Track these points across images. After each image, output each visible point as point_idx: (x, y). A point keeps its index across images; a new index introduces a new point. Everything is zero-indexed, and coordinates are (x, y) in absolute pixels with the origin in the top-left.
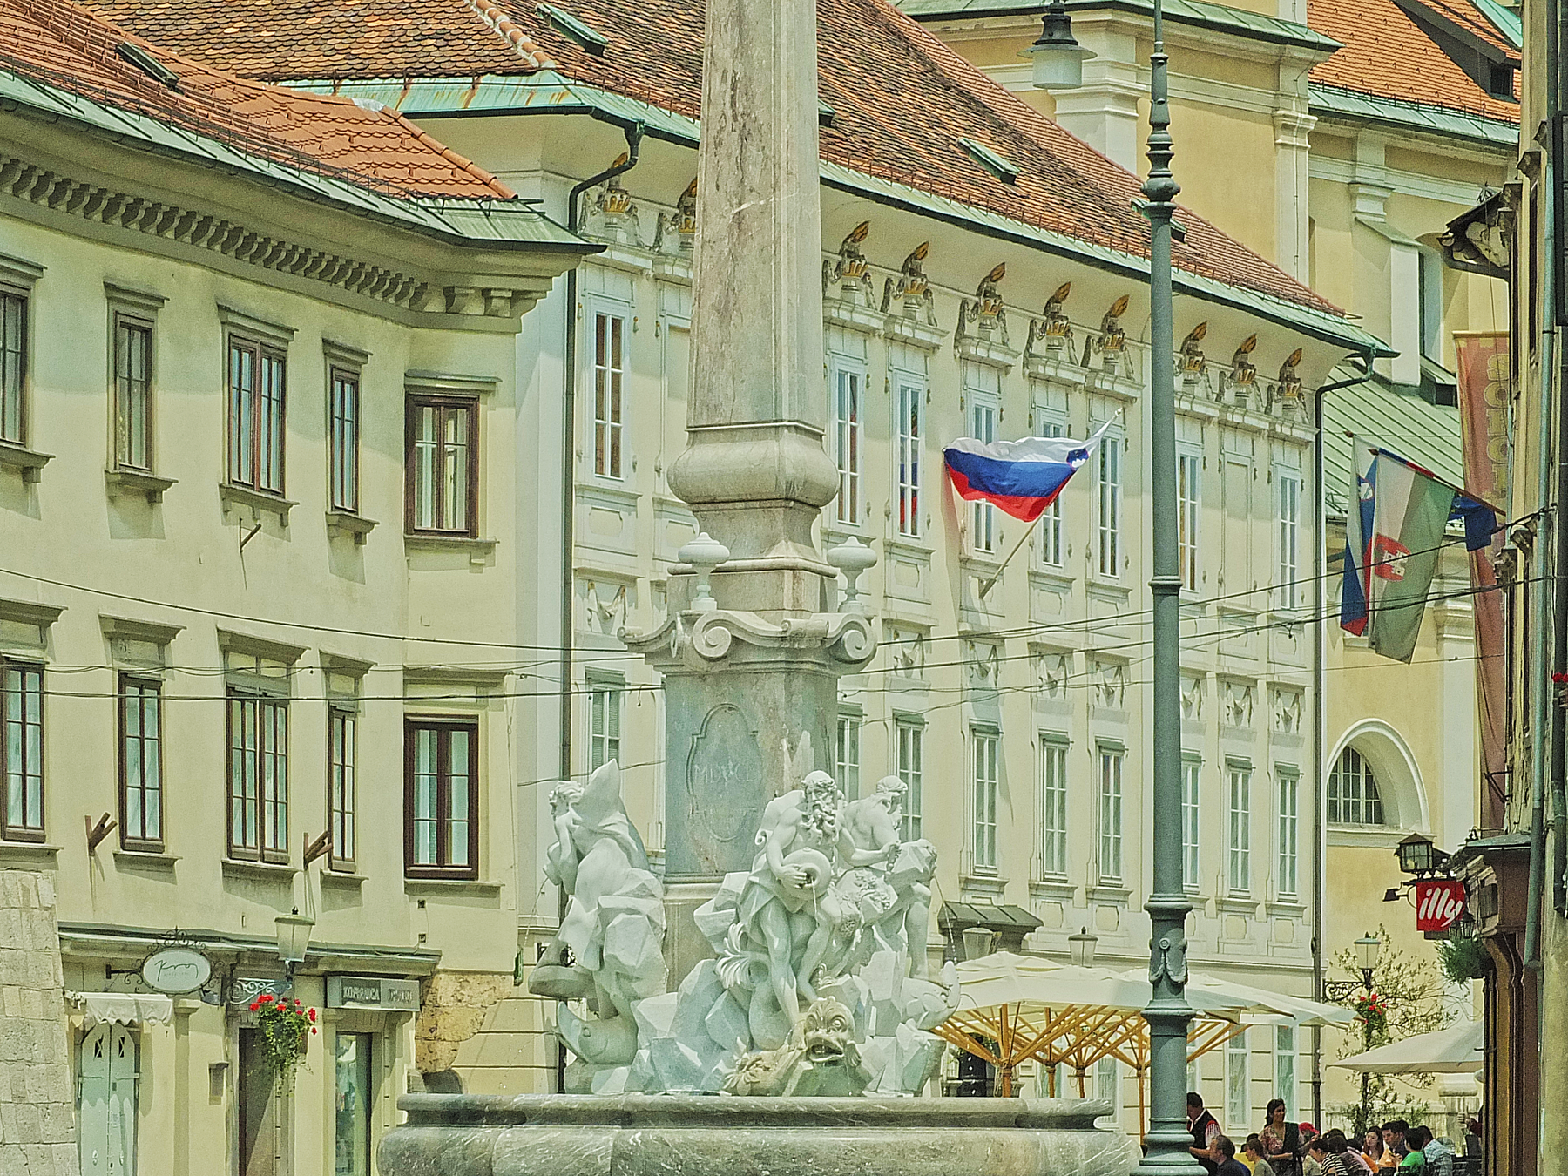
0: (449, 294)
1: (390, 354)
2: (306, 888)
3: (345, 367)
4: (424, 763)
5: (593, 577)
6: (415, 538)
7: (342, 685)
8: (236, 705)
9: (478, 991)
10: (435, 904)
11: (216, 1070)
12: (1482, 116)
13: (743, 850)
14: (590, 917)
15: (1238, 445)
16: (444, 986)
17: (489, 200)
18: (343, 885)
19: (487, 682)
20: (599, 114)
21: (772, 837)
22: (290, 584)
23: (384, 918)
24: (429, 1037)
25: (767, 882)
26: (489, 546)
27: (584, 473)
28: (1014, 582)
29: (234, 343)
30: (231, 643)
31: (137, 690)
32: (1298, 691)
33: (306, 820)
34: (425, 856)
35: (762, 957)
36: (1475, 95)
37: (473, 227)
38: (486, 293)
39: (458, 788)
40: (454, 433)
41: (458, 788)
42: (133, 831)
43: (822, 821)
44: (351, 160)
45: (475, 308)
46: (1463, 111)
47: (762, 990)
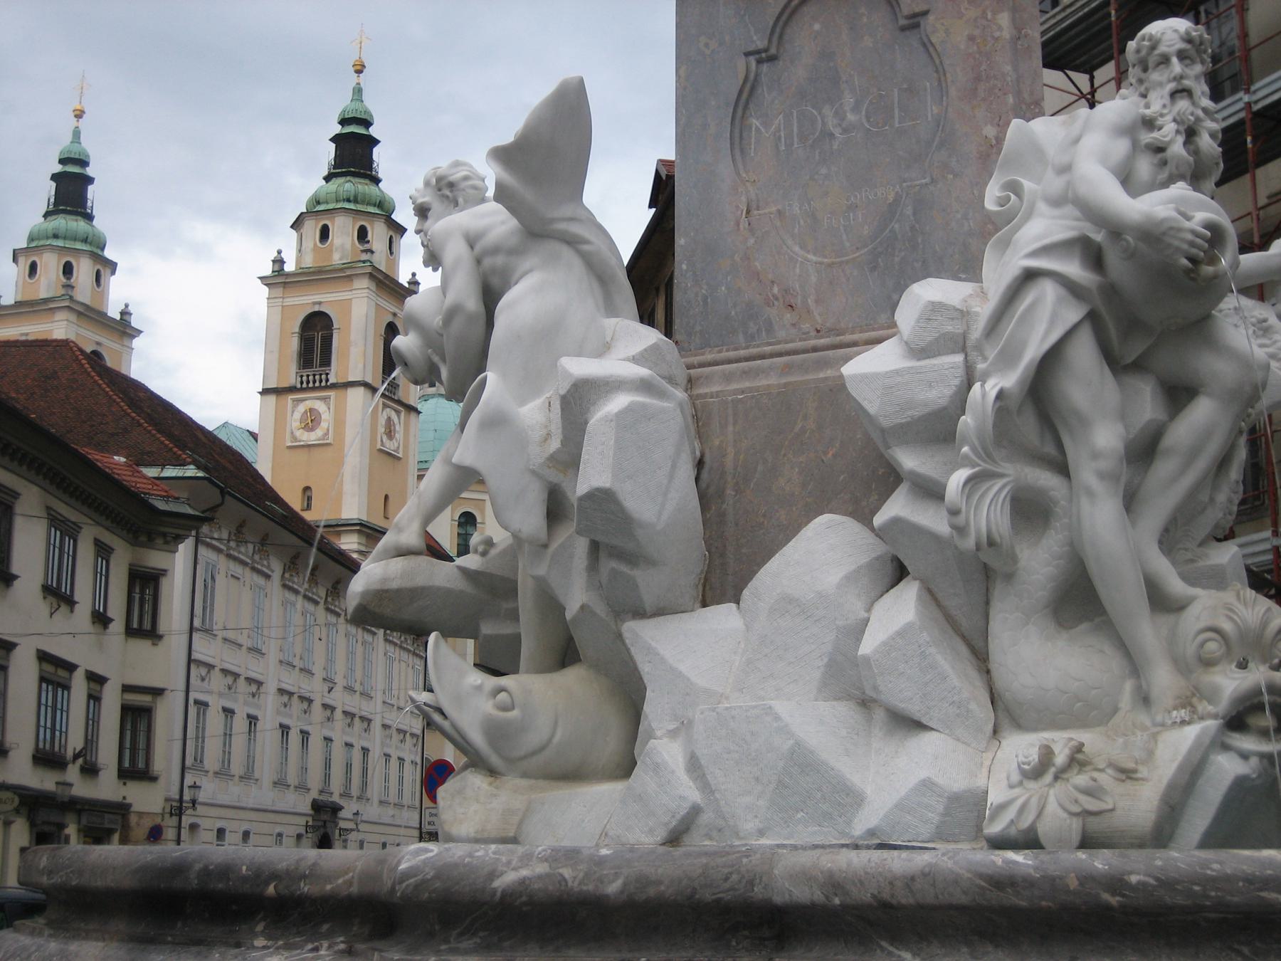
2: (73, 773)
6: (130, 632)
7: (94, 686)
8: (44, 685)
10: (130, 784)
14: (535, 414)
15: (405, 655)
16: (133, 819)
18: (90, 770)
19: (157, 692)
22: (72, 637)
23: (107, 788)
25: (1073, 268)
26: (160, 637)
28: (338, 689)
30: (43, 657)
33: (75, 741)
35: (1046, 479)
37: (161, 505)
38: (164, 535)
45: (160, 541)
47: (1039, 562)
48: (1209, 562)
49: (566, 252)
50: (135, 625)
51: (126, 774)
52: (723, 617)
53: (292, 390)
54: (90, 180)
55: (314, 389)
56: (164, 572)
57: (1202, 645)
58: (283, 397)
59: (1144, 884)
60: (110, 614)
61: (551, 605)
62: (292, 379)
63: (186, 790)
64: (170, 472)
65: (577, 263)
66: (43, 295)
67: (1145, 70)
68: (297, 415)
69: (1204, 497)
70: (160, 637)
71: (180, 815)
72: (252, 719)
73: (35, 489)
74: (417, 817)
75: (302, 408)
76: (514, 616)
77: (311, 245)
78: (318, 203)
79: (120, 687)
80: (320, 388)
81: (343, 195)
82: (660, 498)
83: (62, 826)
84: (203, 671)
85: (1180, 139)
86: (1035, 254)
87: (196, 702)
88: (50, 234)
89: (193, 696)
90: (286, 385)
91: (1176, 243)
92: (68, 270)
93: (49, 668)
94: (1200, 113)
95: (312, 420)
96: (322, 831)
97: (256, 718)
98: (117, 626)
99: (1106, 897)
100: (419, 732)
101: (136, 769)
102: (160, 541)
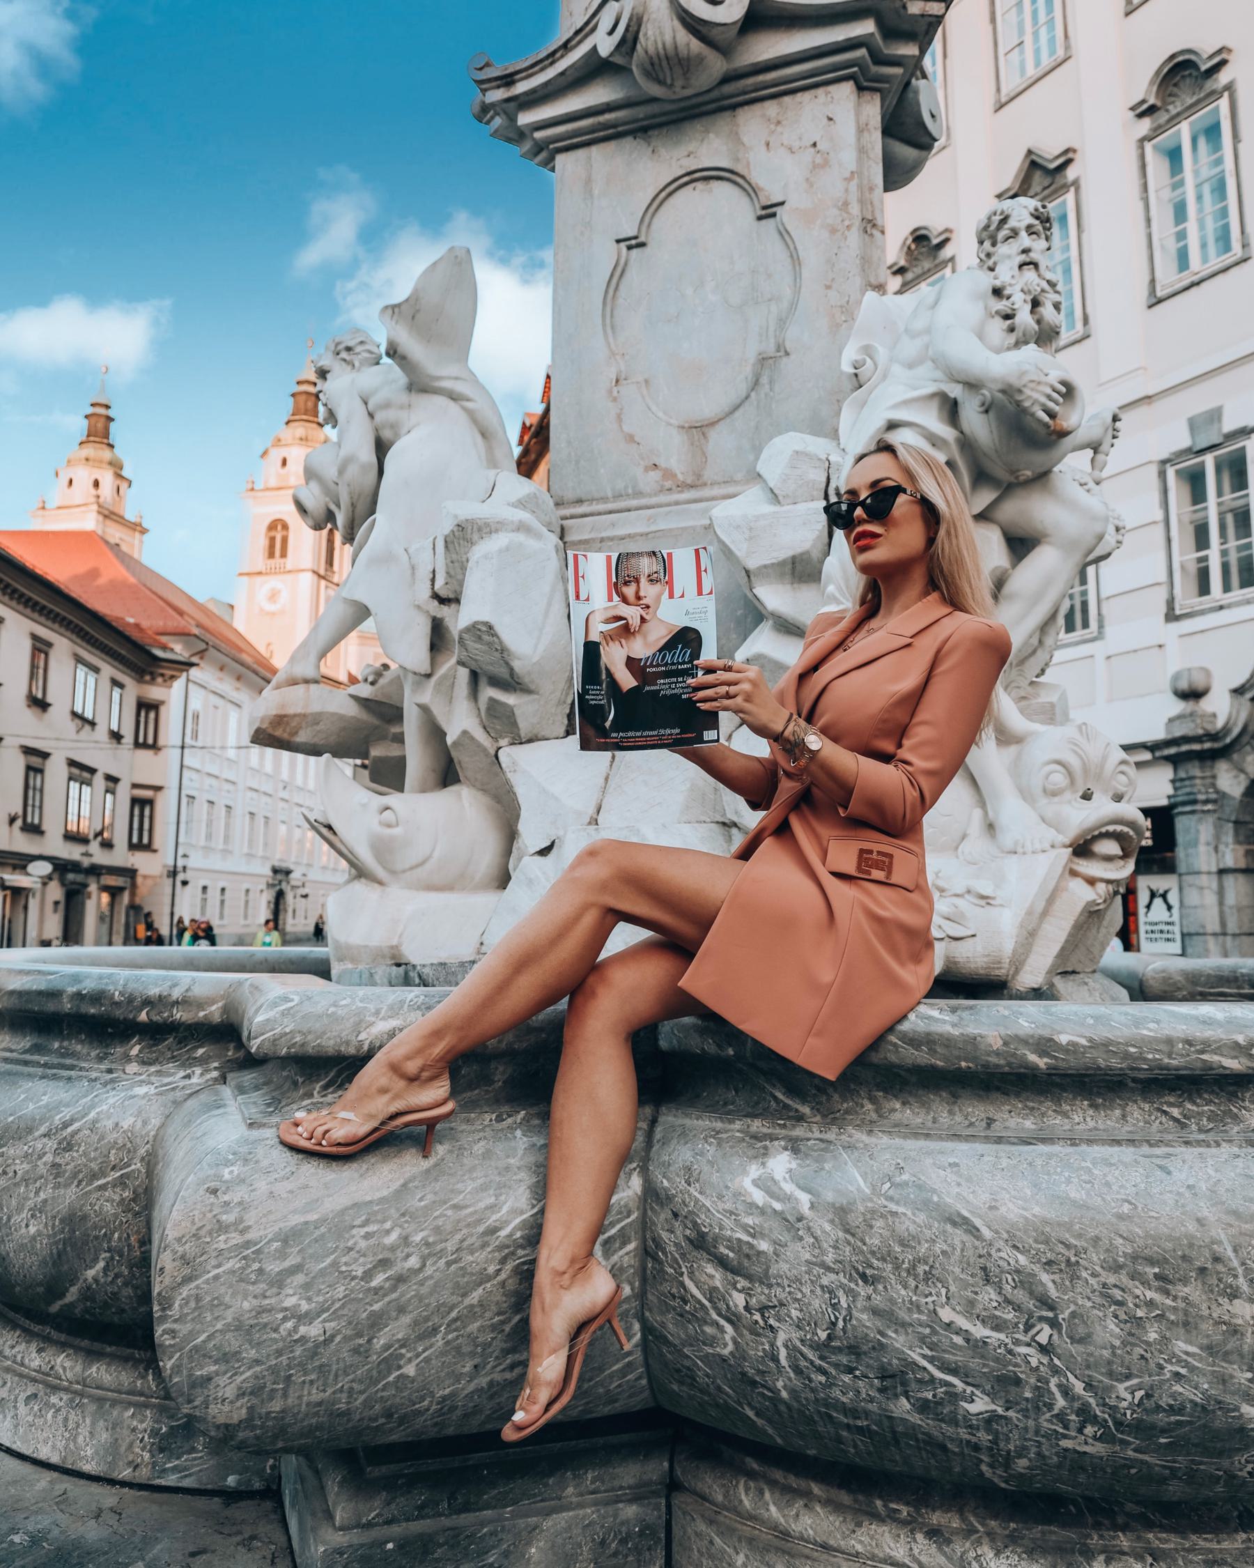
0: (152, 674)
1: (133, 691)
2: (94, 847)
6: (137, 745)
7: (111, 785)
9: (149, 882)
16: (139, 880)
17: (164, 648)
18: (107, 845)
19: (158, 789)
23: (120, 856)
24: (133, 894)
27: (188, 740)
30: (72, 763)
34: (135, 840)
37: (159, 653)
38: (162, 675)
40: (152, 715)
42: (29, 820)
43: (1036, 303)
45: (160, 680)
48: (1040, 700)
49: (453, 407)
51: (133, 847)
56: (163, 703)
57: (1047, 777)
59: (1075, 1044)
60: (122, 732)
61: (435, 733)
65: (463, 418)
67: (994, 244)
69: (1035, 641)
73: (65, 641)
76: (399, 739)
79: (129, 786)
83: (86, 886)
85: (1028, 307)
86: (897, 406)
89: (184, 793)
91: (1036, 395)
93: (76, 771)
94: (1045, 285)
96: (278, 888)
99: (1033, 1058)
101: (141, 845)
102: (160, 680)
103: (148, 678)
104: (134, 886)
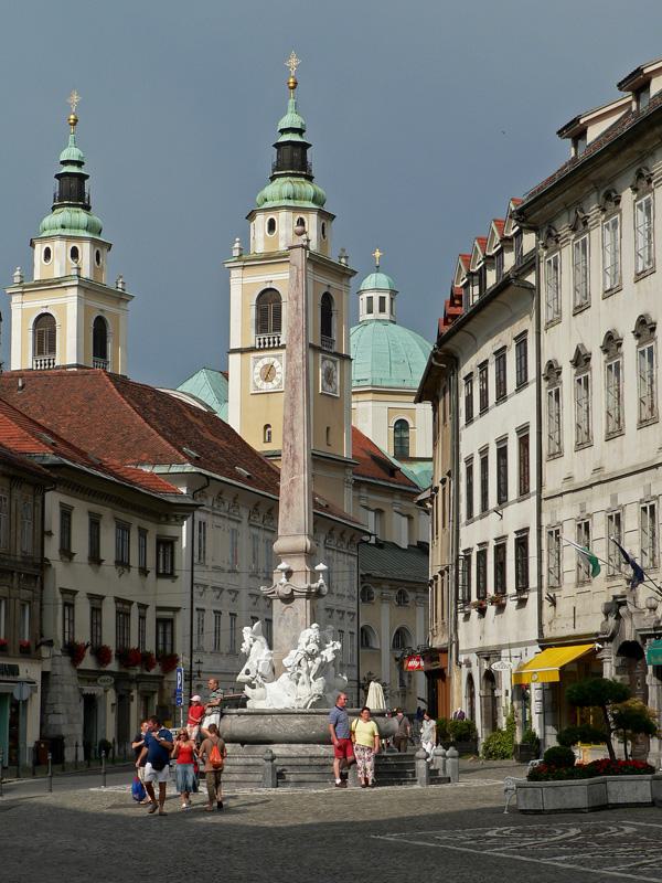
0: (167, 515)
1: (153, 531)
3: (143, 533)
4: (161, 630)
5: (198, 585)
6: (159, 575)
7: (142, 611)
11: (113, 705)
12: (389, 481)
13: (295, 645)
14: (255, 663)
15: (341, 556)
19: (176, 610)
20: (201, 473)
21: (303, 640)
26: (176, 577)
27: (196, 560)
29: (118, 527)
30: (118, 600)
31: (96, 611)
32: (354, 614)
36: (387, 477)
37: (173, 500)
38: (176, 516)
39: (169, 636)
41: (169, 636)
44: (144, 483)
45: (173, 520)
46: (384, 480)
50: (161, 571)
52: (275, 683)
53: (252, 350)
54: (87, 177)
55: (269, 349)
58: (246, 355)
62: (252, 341)
63: (194, 665)
64: (175, 469)
66: (57, 274)
68: (258, 370)
70: (176, 577)
71: (191, 681)
72: (233, 615)
73: (109, 509)
74: (356, 672)
75: (260, 364)
77: (262, 235)
78: (266, 200)
80: (274, 348)
81: (285, 194)
82: (267, 671)
83: (130, 691)
84: (201, 589)
87: (198, 609)
88: (59, 225)
89: (196, 605)
90: (249, 346)
92: (75, 253)
93: (119, 605)
95: (268, 373)
97: (235, 615)
98: (152, 575)
100: (355, 610)
103: (163, 519)
104: (162, 690)
